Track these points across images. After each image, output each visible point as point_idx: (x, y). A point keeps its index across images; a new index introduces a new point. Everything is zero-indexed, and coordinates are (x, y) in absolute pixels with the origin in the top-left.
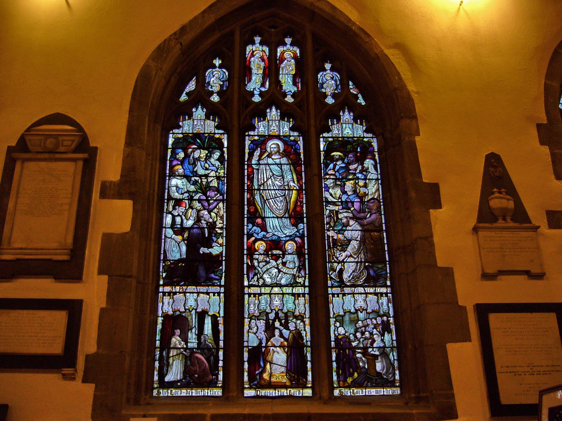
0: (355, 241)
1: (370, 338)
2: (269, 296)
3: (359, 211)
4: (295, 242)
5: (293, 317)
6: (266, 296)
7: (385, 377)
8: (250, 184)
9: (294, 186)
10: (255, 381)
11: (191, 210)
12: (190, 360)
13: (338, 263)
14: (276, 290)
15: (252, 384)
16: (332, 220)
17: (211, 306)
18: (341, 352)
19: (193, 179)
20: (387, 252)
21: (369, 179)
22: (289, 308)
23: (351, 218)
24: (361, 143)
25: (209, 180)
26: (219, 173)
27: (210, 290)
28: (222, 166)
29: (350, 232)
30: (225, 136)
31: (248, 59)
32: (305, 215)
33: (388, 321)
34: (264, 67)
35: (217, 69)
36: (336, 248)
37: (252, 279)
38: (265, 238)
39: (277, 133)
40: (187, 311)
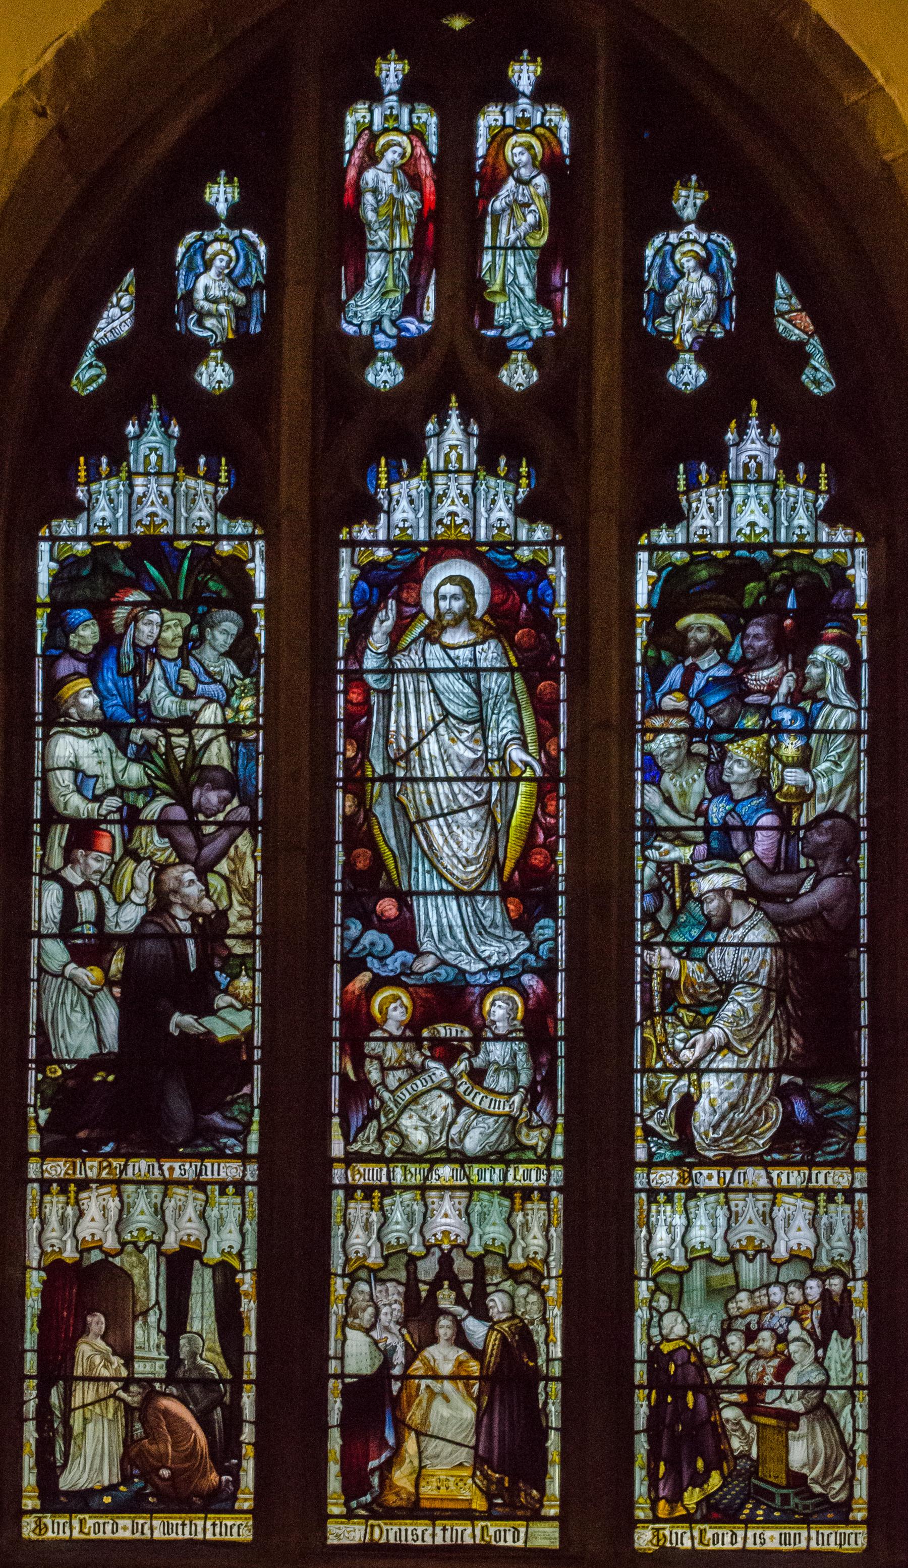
0: (749, 990)
1: (776, 1354)
2: (419, 1197)
3: (770, 866)
4: (523, 992)
5: (504, 1273)
6: (407, 1196)
7: (817, 1489)
8: (356, 756)
9: (526, 764)
10: (365, 1495)
11: (131, 865)
12: (144, 1423)
13: (679, 1073)
14: (445, 1172)
15: (354, 1504)
16: (666, 903)
17: (214, 1232)
18: (669, 1399)
19: (136, 735)
20: (865, 1032)
21: (823, 731)
22: (490, 1242)
23: (738, 895)
24: (803, 572)
25: (198, 743)
26: (237, 711)
27: (209, 1173)
28: (247, 681)
29: (732, 949)
30: (257, 548)
31: (352, 173)
32: (561, 887)
33: (846, 1293)
34: (419, 214)
35: (223, 230)
36: (671, 1014)
37: (357, 1134)
38: (408, 975)
39: (465, 530)
40: (130, 1248)
